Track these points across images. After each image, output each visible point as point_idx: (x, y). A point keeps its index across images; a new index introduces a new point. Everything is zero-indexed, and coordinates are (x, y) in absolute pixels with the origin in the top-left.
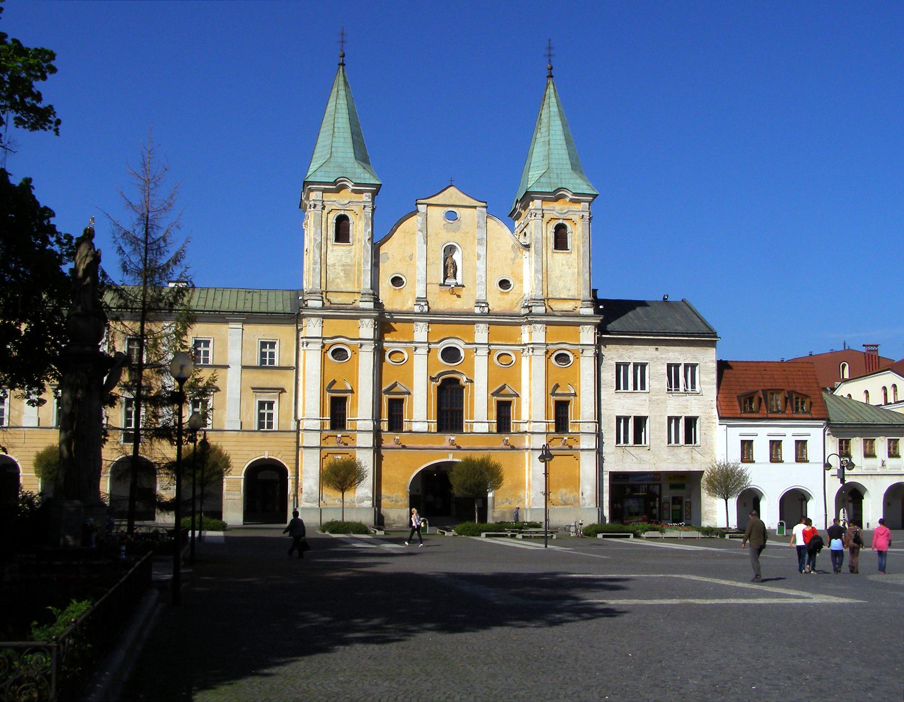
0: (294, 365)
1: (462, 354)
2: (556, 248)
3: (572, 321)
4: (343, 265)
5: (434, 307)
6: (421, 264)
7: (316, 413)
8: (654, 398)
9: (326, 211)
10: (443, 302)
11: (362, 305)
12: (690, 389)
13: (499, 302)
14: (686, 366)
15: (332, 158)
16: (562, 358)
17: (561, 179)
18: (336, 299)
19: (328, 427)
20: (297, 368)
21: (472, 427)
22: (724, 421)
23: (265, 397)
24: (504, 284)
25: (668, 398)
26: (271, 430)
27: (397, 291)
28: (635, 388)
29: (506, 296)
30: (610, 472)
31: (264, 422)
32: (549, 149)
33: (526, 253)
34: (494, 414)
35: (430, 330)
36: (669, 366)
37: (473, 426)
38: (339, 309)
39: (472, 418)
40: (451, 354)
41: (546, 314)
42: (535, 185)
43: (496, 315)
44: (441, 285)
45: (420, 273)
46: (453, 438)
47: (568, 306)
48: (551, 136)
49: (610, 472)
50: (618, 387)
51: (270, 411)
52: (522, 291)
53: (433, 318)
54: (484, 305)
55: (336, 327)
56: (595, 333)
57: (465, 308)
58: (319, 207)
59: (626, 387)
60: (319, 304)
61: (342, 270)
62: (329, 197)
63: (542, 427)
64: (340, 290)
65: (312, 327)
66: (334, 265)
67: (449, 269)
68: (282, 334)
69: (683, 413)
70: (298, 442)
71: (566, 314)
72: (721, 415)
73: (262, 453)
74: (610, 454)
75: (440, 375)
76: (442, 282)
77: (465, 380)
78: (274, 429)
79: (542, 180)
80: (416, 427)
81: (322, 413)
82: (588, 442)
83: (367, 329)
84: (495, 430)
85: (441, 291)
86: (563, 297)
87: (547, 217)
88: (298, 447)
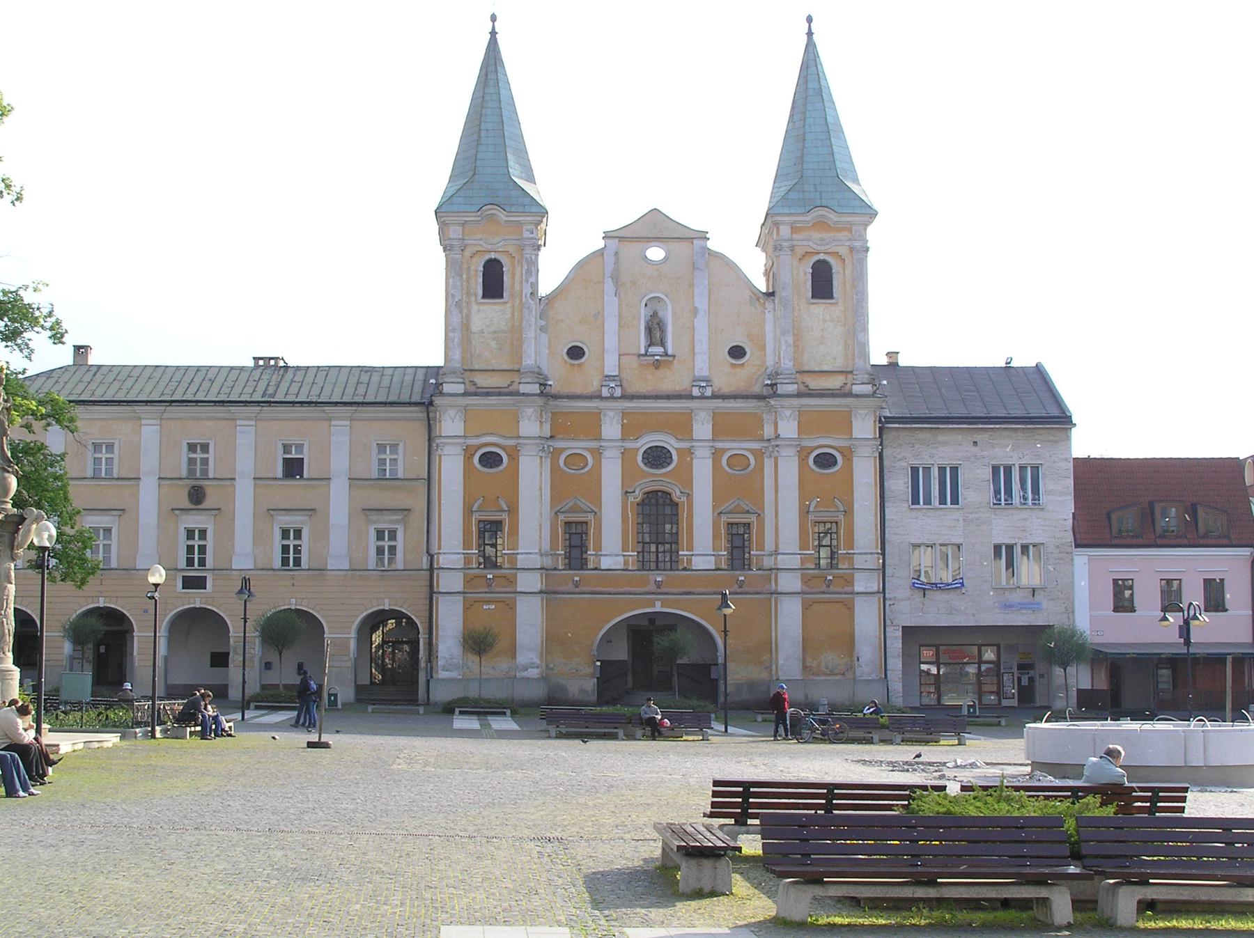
0: (426, 477)
1: (675, 457)
2: (814, 296)
4: (495, 332)
5: (631, 389)
6: (611, 326)
7: (618, 549)
8: (971, 516)
9: (468, 253)
11: (523, 389)
12: (1030, 502)
13: (728, 377)
14: (1022, 469)
15: (477, 176)
16: (826, 461)
17: (821, 192)
18: (483, 381)
21: (689, 561)
24: (737, 352)
25: (993, 517)
26: (288, 568)
27: (568, 366)
28: (943, 501)
29: (738, 370)
30: (903, 627)
31: (290, 558)
32: (804, 147)
33: (769, 305)
34: (724, 542)
35: (625, 421)
36: (995, 469)
37: (691, 559)
38: (488, 394)
39: (690, 548)
41: (799, 395)
42: (780, 204)
43: (724, 397)
44: (640, 355)
45: (611, 341)
46: (659, 579)
47: (835, 383)
48: (806, 127)
49: (903, 627)
50: (915, 501)
51: (202, 543)
52: (764, 362)
54: (703, 384)
56: (875, 421)
57: (677, 388)
59: (928, 501)
60: (460, 389)
61: (494, 339)
64: (491, 368)
65: (451, 424)
66: (482, 331)
67: (655, 331)
69: (1019, 538)
70: (431, 586)
71: (831, 394)
72: (1078, 541)
73: (191, 600)
74: (902, 600)
76: (643, 352)
77: (678, 493)
78: (207, 567)
79: (792, 195)
80: (606, 563)
81: (467, 544)
85: (641, 365)
86: (825, 368)
87: (800, 251)
88: (432, 592)
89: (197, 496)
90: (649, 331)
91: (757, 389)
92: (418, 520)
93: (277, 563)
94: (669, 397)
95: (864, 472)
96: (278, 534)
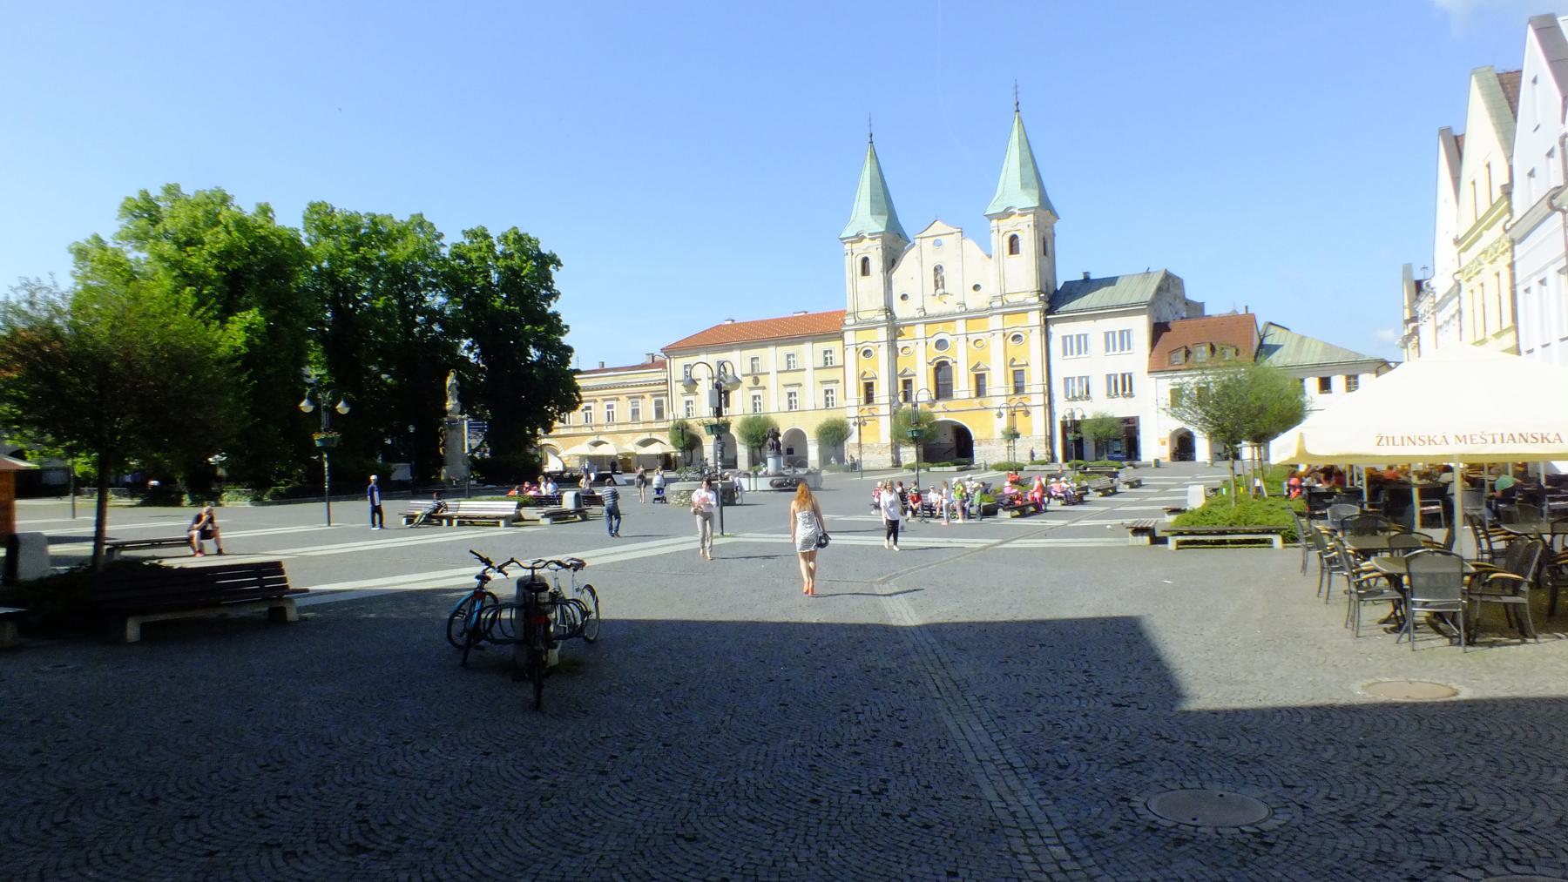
3: (1021, 310)
10: (934, 307)
19: (862, 402)
20: (843, 366)
22: (1152, 375)
23: (828, 387)
24: (976, 287)
36: (1107, 334)
40: (941, 344)
50: (1065, 354)
53: (928, 320)
55: (863, 336)
58: (850, 254)
62: (855, 246)
63: (1003, 392)
65: (849, 337)
68: (835, 345)
75: (934, 360)
82: (1040, 399)
83: (882, 334)
84: (973, 395)
89: (756, 381)
90: (936, 281)
91: (988, 306)
92: (841, 383)
93: (786, 408)
94: (944, 316)
95: (1035, 340)
96: (823, 393)
